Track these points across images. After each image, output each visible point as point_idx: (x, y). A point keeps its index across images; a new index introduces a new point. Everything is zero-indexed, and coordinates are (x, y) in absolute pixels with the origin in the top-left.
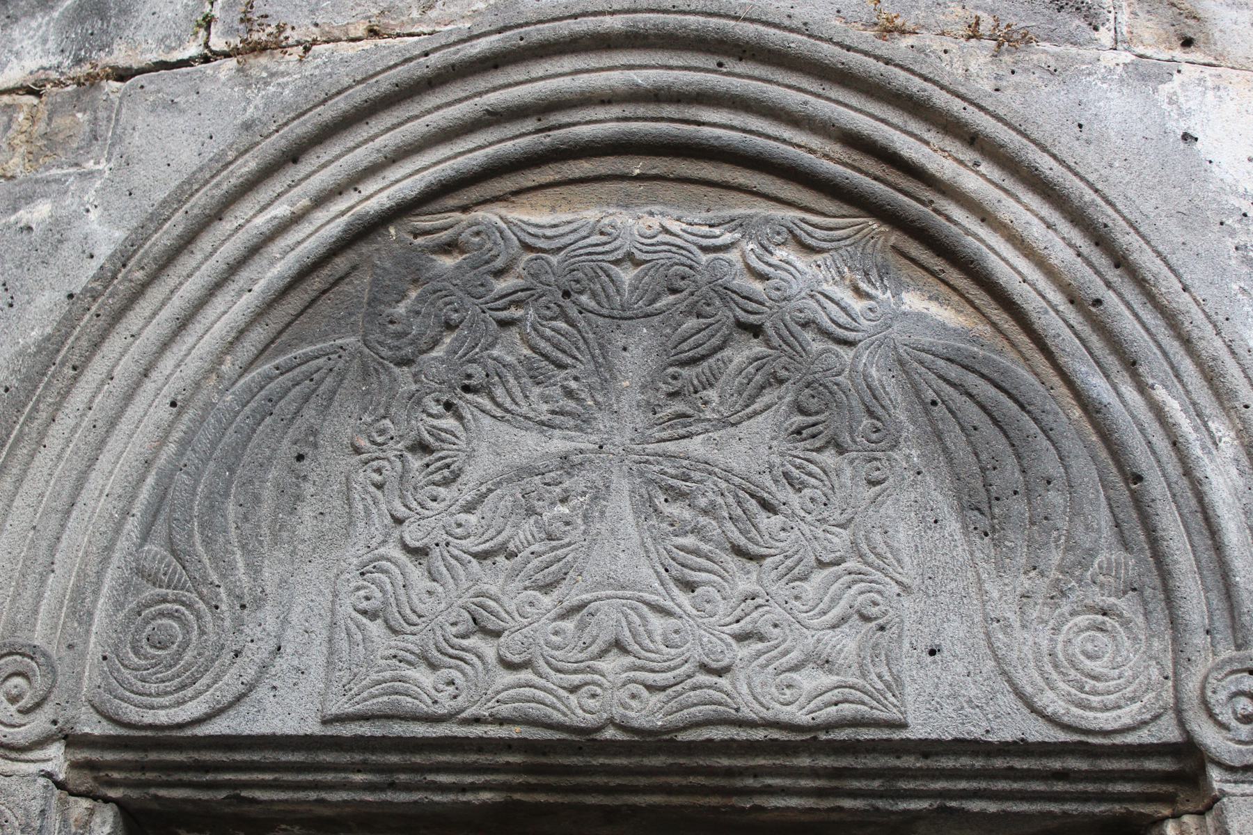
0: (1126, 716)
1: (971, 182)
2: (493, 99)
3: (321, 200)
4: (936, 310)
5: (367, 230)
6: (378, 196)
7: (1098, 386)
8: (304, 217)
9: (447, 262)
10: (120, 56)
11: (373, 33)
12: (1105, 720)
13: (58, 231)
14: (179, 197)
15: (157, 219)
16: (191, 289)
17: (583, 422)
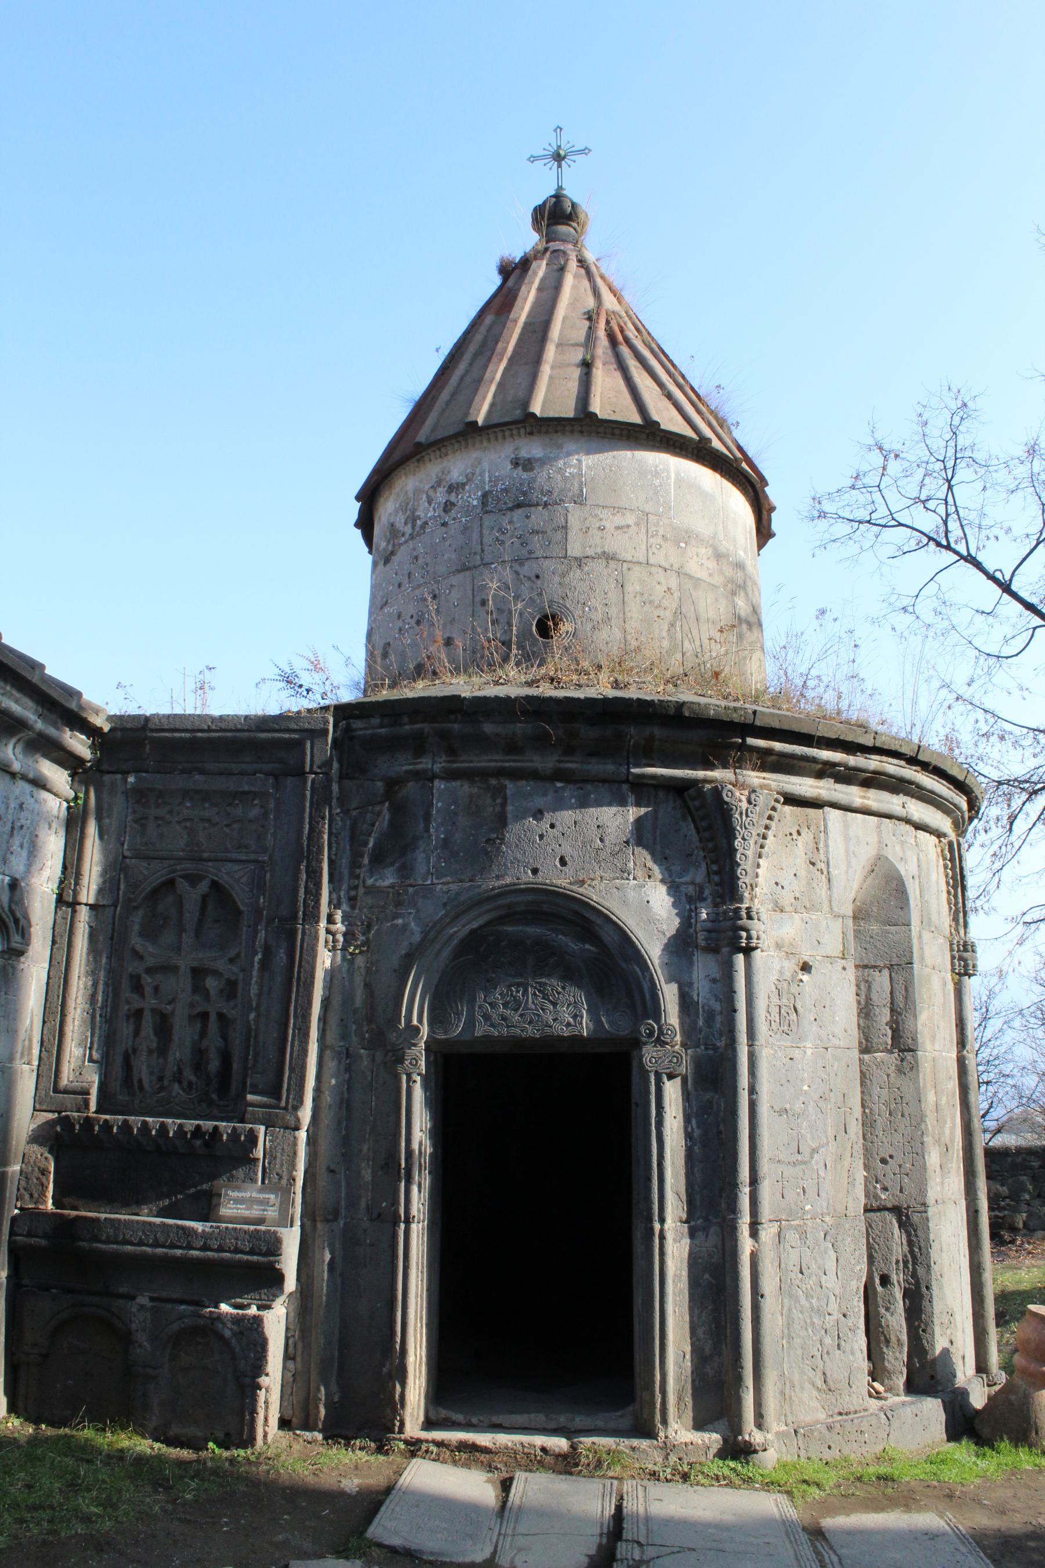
0: (626, 1033)
1: (599, 921)
2: (499, 903)
3: (464, 926)
4: (592, 948)
5: (473, 932)
6: (475, 925)
7: (624, 965)
8: (460, 930)
9: (491, 938)
10: (411, 881)
11: (470, 881)
12: (622, 1033)
13: (405, 927)
14: (433, 927)
15: (429, 931)
16: (438, 947)
17: (521, 976)
